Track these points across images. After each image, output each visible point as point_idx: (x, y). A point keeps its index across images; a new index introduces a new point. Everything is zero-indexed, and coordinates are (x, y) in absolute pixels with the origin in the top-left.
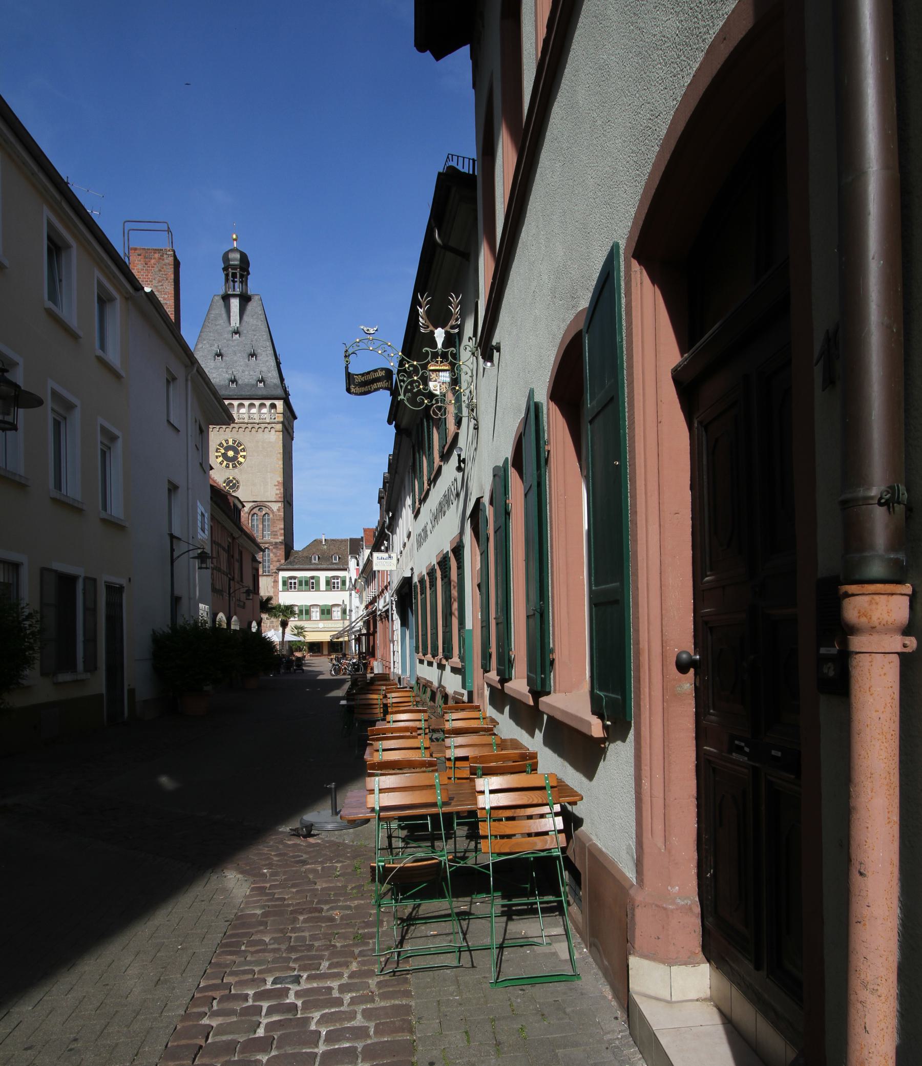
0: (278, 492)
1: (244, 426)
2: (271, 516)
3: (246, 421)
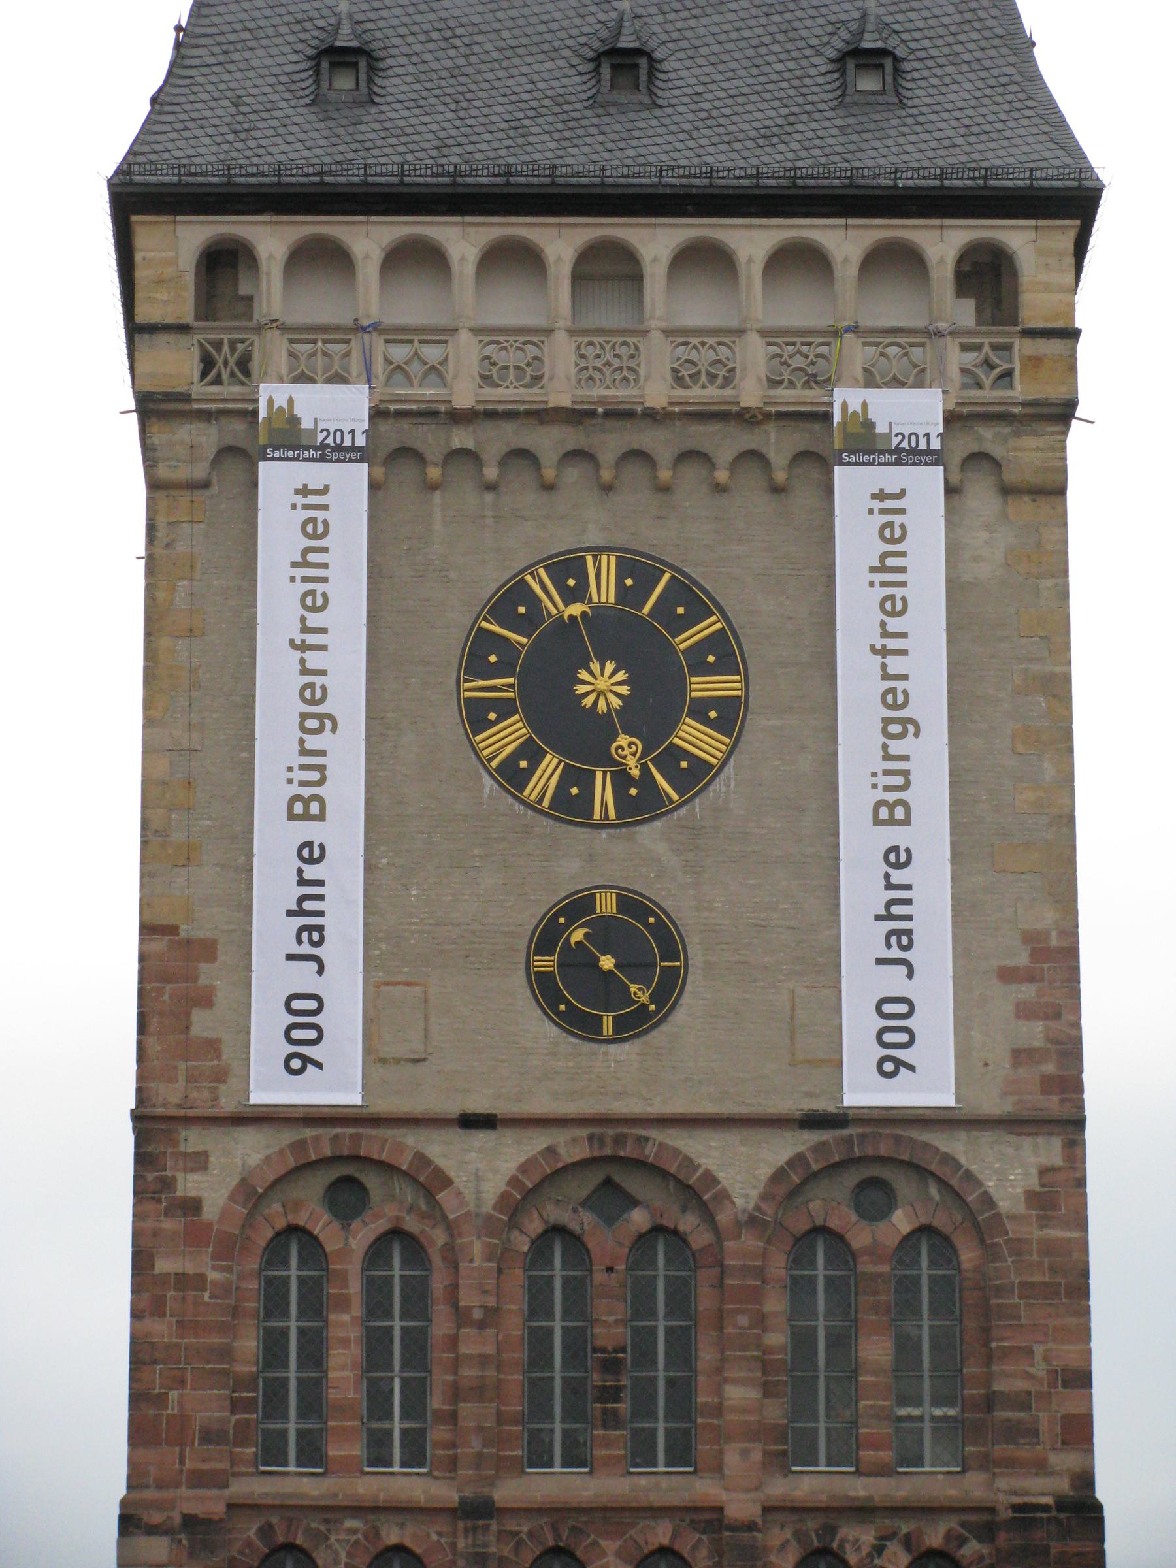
0: (1034, 1033)
1: (725, 445)
2: (968, 1255)
3: (750, 393)
